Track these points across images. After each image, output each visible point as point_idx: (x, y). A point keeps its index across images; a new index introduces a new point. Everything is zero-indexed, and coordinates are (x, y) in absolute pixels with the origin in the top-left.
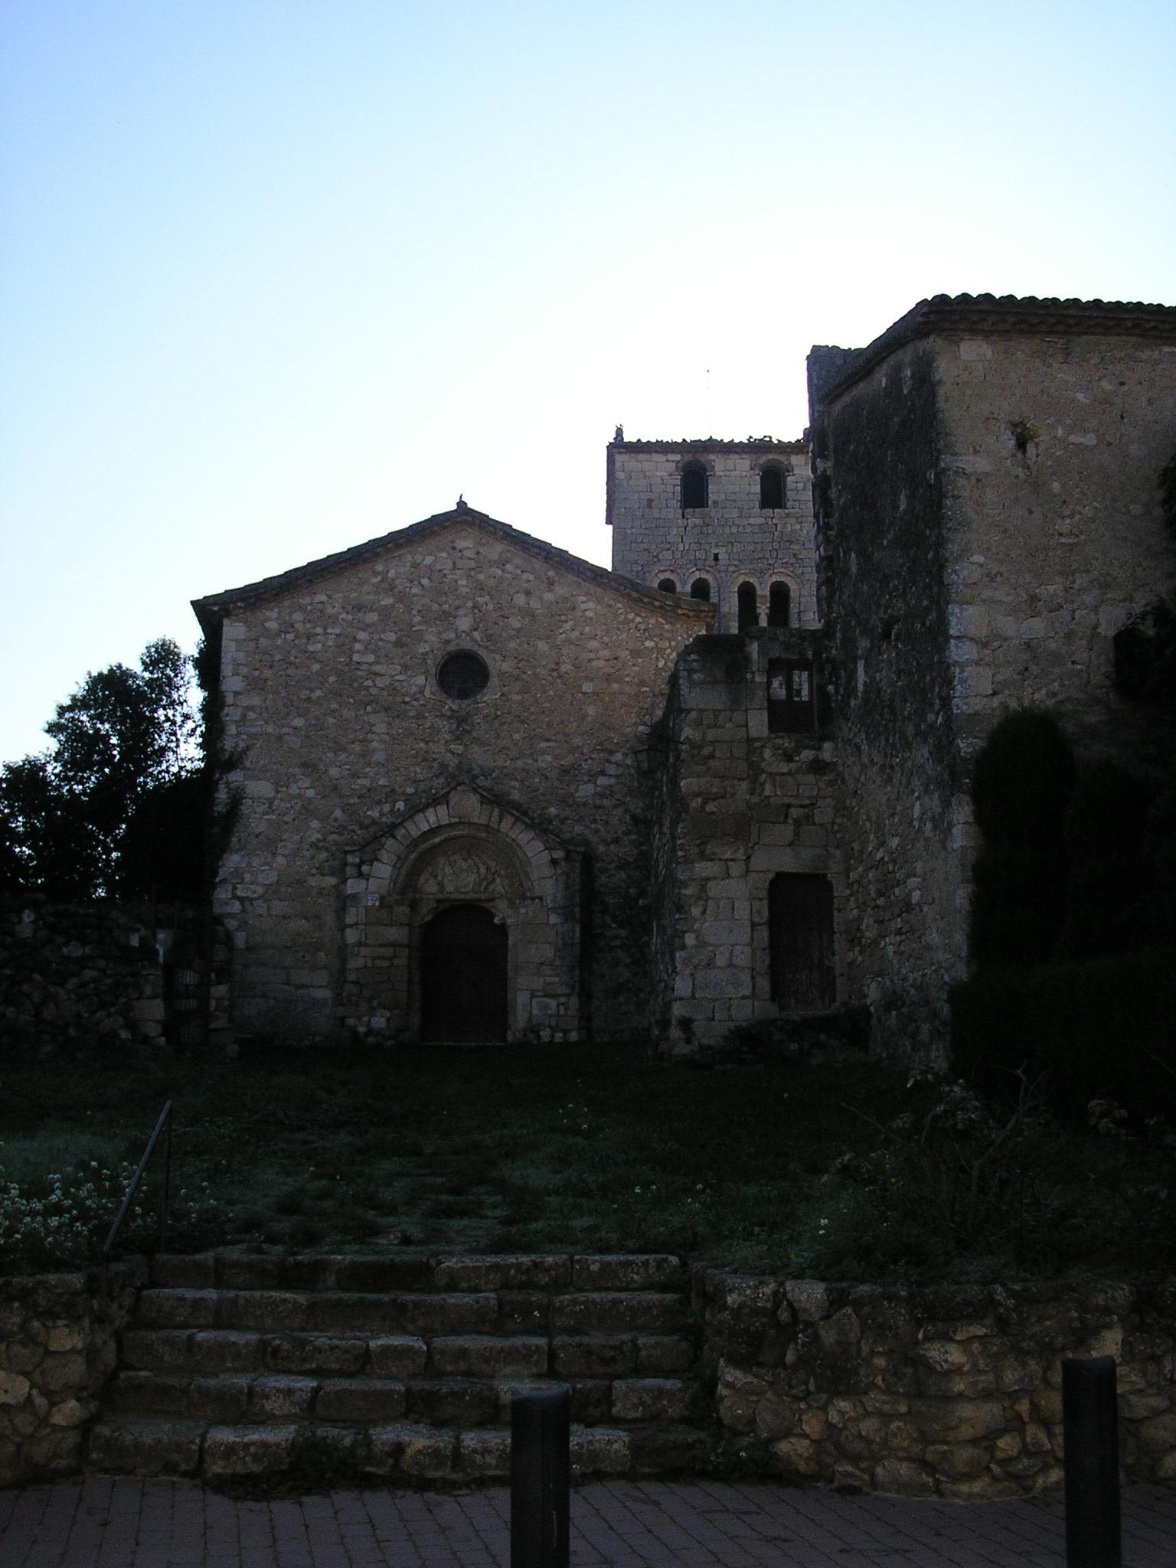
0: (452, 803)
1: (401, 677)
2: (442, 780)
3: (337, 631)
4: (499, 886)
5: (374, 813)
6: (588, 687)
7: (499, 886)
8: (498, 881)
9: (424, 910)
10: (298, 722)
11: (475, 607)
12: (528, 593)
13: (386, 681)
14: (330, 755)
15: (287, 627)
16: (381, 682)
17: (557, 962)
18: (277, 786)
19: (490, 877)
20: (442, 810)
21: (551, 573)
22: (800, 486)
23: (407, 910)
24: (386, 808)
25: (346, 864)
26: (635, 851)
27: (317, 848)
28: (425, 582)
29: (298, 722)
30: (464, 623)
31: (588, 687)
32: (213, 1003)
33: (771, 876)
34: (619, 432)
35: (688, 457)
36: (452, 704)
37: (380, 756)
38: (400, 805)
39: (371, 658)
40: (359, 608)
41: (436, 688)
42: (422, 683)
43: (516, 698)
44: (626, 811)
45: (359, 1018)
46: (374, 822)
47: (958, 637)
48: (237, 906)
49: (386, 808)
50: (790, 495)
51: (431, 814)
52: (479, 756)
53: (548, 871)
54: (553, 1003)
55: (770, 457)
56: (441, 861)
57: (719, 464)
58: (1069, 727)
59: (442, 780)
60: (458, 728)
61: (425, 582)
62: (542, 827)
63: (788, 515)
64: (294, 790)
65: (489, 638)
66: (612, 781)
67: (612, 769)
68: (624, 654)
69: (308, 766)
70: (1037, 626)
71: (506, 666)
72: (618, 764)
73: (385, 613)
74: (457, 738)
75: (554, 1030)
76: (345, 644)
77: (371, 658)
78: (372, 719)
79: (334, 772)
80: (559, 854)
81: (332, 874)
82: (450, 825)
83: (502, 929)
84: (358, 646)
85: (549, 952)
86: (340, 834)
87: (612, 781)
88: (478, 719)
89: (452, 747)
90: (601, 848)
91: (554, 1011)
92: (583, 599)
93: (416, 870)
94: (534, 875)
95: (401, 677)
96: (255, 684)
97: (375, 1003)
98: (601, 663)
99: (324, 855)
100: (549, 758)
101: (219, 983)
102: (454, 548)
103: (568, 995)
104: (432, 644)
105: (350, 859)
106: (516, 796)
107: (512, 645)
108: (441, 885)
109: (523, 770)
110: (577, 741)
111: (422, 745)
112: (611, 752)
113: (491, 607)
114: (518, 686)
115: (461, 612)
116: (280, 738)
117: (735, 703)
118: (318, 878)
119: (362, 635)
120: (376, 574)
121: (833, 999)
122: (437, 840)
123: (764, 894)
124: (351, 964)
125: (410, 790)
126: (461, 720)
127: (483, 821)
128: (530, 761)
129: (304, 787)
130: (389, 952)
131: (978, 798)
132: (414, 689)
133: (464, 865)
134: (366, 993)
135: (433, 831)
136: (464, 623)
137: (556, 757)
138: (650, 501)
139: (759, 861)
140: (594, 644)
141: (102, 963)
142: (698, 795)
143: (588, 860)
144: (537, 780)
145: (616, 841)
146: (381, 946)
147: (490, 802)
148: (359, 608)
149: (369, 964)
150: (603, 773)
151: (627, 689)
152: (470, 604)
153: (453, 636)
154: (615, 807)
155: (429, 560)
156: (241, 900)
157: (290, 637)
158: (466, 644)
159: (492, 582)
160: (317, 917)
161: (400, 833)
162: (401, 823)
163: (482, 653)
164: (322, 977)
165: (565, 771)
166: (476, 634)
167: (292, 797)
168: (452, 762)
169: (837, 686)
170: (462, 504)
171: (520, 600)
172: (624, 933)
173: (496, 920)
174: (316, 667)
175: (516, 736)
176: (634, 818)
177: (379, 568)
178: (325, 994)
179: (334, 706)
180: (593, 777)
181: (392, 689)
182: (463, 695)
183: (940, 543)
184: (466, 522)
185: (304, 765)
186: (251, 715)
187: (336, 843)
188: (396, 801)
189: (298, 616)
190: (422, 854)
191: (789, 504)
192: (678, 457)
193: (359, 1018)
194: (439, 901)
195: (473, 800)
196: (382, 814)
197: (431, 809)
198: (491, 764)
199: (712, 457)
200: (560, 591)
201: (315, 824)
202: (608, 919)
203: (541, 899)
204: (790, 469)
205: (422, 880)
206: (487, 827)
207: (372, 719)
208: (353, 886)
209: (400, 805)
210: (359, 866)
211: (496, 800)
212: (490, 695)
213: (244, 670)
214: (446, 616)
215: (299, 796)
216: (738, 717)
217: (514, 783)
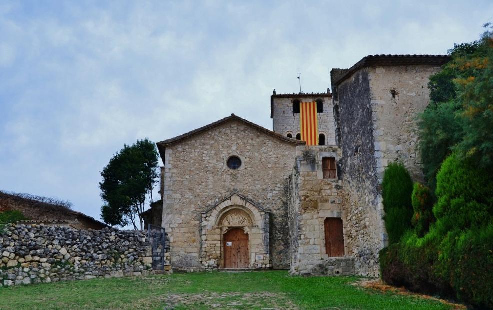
0: (232, 199)
1: (217, 164)
2: (229, 193)
3: (199, 151)
5: (210, 203)
6: (270, 166)
7: (246, 223)
8: (246, 221)
9: (225, 230)
10: (188, 177)
11: (237, 143)
12: (252, 139)
13: (213, 165)
14: (197, 186)
16: (211, 165)
17: (263, 244)
19: (243, 220)
20: (229, 201)
21: (259, 134)
22: (327, 106)
23: (220, 230)
24: (213, 201)
25: (202, 217)
26: (285, 212)
27: (194, 213)
28: (223, 136)
29: (188, 177)
30: (234, 148)
31: (270, 166)
32: (165, 258)
33: (325, 218)
34: (275, 92)
35: (295, 99)
36: (232, 171)
37: (211, 186)
38: (217, 200)
39: (208, 158)
41: (227, 166)
43: (250, 169)
44: (282, 200)
45: (206, 261)
46: (210, 205)
47: (378, 151)
48: (170, 230)
49: (213, 201)
50: (324, 109)
51: (226, 202)
52: (239, 186)
53: (260, 218)
54: (262, 256)
55: (318, 98)
56: (229, 216)
58: (411, 175)
59: (229, 193)
60: (233, 178)
61: (223, 136)
62: (258, 206)
63: (324, 115)
64: (187, 196)
65: (242, 152)
66: (278, 192)
67: (277, 189)
68: (279, 156)
70: (400, 147)
71: (247, 160)
72: (279, 187)
74: (233, 181)
75: (263, 264)
76: (201, 155)
77: (208, 158)
78: (209, 175)
79: (198, 191)
80: (263, 213)
81: (198, 220)
82: (232, 206)
83: (247, 235)
84: (204, 155)
85: (260, 241)
86: (200, 209)
87: (278, 192)
88: (238, 175)
89: (232, 183)
90: (275, 212)
91: (263, 259)
92: (268, 140)
93: (222, 219)
94: (256, 219)
95: (217, 164)
97: (211, 257)
98: (273, 159)
99: (195, 215)
100: (259, 186)
101: (167, 252)
102: (231, 127)
103: (266, 254)
104: (226, 155)
105: (203, 215)
106: (250, 197)
107: (248, 154)
108: (229, 223)
109: (252, 189)
110: (267, 181)
111: (223, 183)
112: (277, 184)
113: (242, 143)
114: (250, 166)
115: (233, 145)
117: (313, 169)
118: (194, 221)
119: (206, 152)
120: (209, 134)
121: (344, 254)
122: (228, 210)
123: (323, 224)
124: (204, 246)
125: (220, 196)
127: (241, 204)
128: (254, 187)
129: (189, 195)
130: (215, 242)
132: (220, 167)
133: (236, 217)
134: (208, 254)
135: (227, 208)
136: (234, 148)
137: (261, 186)
138: (284, 112)
139: (321, 214)
140: (271, 153)
141: (135, 247)
142: (304, 196)
143: (271, 216)
144: (256, 192)
145: (279, 209)
146: (213, 240)
147: (243, 199)
149: (209, 246)
150: (275, 190)
151: (281, 166)
152: (236, 142)
153: (231, 151)
154: (278, 200)
155: (224, 130)
156: (172, 228)
157: (185, 152)
158: (235, 154)
159: (242, 136)
160: (194, 233)
161: (217, 208)
162: (218, 205)
163: (240, 156)
164: (196, 250)
165: (264, 190)
166: (238, 151)
167: (186, 199)
168: (232, 188)
169: (342, 165)
170: (233, 114)
171: (250, 141)
172: (282, 236)
173: (245, 233)
174: (192, 161)
175: (250, 180)
176: (284, 203)
177: (210, 133)
178: (196, 255)
179: (198, 172)
180: (272, 191)
181: (214, 167)
182: (234, 168)
183: (372, 124)
184: (234, 120)
185: (190, 189)
186: (174, 175)
187: (199, 212)
188: (216, 199)
190: (224, 214)
191: (324, 111)
192: (292, 99)
193: (206, 261)
194: (229, 227)
195: (238, 198)
196: (212, 203)
197: (226, 201)
198: (243, 188)
199: (301, 98)
200: (261, 138)
201: (193, 206)
202: (277, 232)
203: (258, 226)
204: (325, 101)
205: (224, 221)
206: (242, 206)
207: (209, 175)
208: (204, 223)
209: (217, 200)
210: (206, 218)
211: (243, 198)
212: (242, 168)
213: (172, 162)
214: (230, 146)
215: (188, 198)
216: (314, 173)
217: (249, 193)
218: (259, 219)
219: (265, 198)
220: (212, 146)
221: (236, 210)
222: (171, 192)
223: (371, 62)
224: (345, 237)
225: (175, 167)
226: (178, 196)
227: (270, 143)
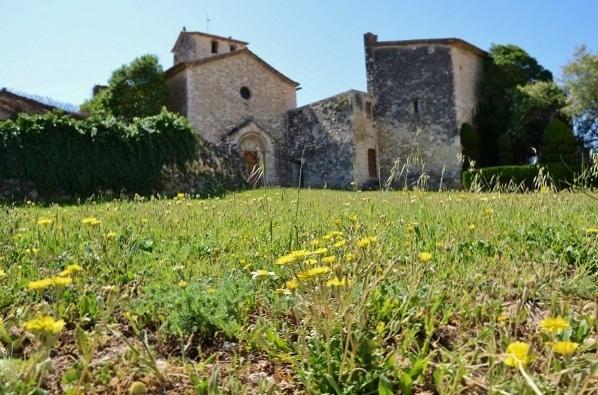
4: (258, 149)
7: (258, 149)
15: (203, 74)
18: (204, 116)
30: (246, 79)
34: (184, 29)
36: (245, 101)
40: (221, 71)
42: (237, 94)
52: (251, 114)
57: (220, 42)
69: (211, 113)
73: (227, 73)
76: (218, 81)
96: (197, 89)
104: (239, 84)
116: (203, 104)
126: (245, 104)
129: (210, 118)
131: (461, 135)
136: (246, 79)
148: (221, 71)
189: (205, 71)
200: (265, 75)
211: (259, 126)
212: (252, 99)
214: (242, 77)
218: (270, 147)
219: (270, 128)
220: (227, 73)
221: (252, 137)
222: (194, 114)
223: (455, 42)
224: (377, 164)
225: (197, 89)
226: (200, 118)
227: (272, 79)
